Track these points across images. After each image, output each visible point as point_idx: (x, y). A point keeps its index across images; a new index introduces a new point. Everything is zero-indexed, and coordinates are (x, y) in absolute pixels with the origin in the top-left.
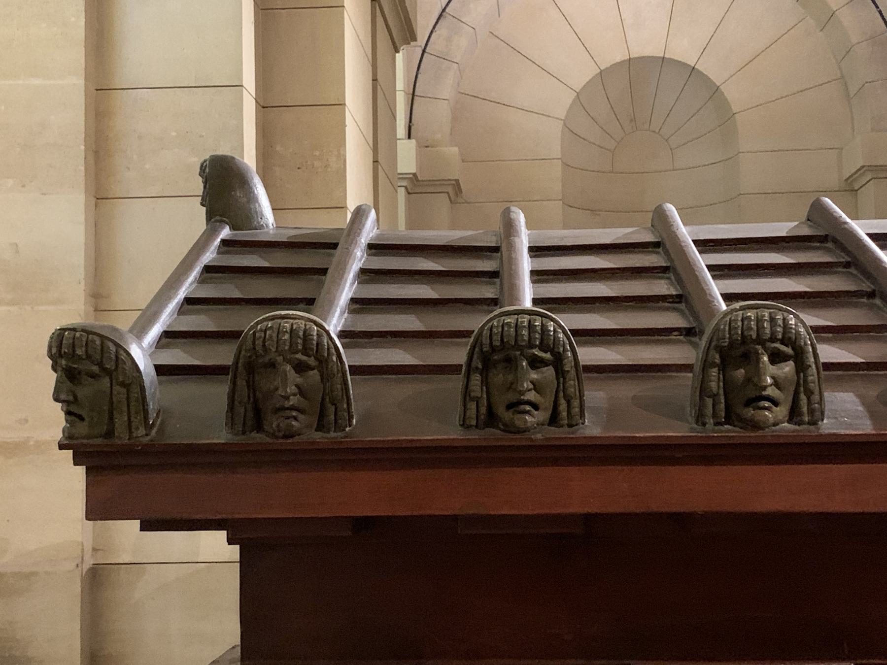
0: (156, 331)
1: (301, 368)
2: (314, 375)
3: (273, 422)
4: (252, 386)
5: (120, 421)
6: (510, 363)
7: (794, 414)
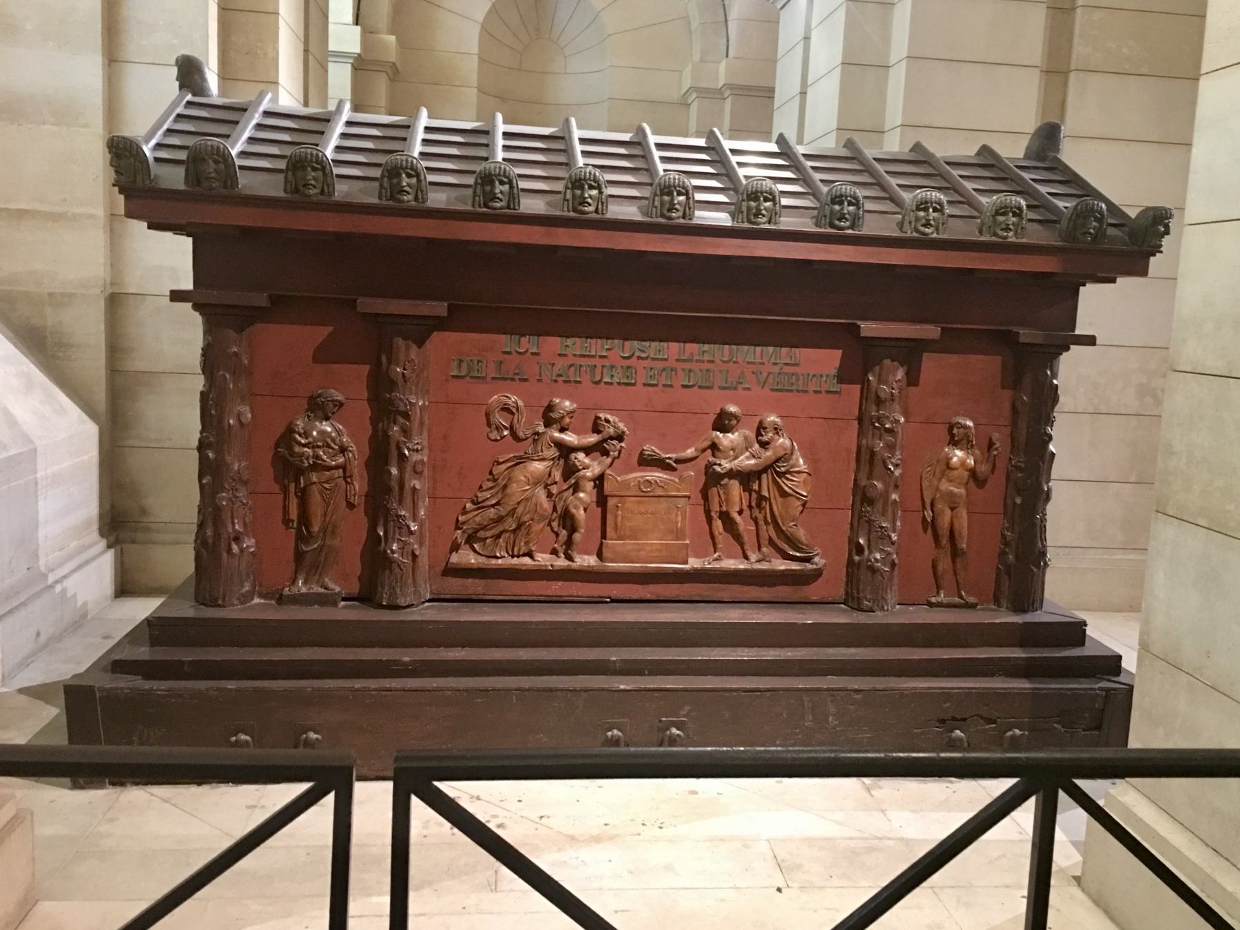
0: (153, 142)
1: (216, 162)
2: (222, 166)
3: (205, 184)
5: (139, 177)
6: (304, 168)
7: (416, 199)
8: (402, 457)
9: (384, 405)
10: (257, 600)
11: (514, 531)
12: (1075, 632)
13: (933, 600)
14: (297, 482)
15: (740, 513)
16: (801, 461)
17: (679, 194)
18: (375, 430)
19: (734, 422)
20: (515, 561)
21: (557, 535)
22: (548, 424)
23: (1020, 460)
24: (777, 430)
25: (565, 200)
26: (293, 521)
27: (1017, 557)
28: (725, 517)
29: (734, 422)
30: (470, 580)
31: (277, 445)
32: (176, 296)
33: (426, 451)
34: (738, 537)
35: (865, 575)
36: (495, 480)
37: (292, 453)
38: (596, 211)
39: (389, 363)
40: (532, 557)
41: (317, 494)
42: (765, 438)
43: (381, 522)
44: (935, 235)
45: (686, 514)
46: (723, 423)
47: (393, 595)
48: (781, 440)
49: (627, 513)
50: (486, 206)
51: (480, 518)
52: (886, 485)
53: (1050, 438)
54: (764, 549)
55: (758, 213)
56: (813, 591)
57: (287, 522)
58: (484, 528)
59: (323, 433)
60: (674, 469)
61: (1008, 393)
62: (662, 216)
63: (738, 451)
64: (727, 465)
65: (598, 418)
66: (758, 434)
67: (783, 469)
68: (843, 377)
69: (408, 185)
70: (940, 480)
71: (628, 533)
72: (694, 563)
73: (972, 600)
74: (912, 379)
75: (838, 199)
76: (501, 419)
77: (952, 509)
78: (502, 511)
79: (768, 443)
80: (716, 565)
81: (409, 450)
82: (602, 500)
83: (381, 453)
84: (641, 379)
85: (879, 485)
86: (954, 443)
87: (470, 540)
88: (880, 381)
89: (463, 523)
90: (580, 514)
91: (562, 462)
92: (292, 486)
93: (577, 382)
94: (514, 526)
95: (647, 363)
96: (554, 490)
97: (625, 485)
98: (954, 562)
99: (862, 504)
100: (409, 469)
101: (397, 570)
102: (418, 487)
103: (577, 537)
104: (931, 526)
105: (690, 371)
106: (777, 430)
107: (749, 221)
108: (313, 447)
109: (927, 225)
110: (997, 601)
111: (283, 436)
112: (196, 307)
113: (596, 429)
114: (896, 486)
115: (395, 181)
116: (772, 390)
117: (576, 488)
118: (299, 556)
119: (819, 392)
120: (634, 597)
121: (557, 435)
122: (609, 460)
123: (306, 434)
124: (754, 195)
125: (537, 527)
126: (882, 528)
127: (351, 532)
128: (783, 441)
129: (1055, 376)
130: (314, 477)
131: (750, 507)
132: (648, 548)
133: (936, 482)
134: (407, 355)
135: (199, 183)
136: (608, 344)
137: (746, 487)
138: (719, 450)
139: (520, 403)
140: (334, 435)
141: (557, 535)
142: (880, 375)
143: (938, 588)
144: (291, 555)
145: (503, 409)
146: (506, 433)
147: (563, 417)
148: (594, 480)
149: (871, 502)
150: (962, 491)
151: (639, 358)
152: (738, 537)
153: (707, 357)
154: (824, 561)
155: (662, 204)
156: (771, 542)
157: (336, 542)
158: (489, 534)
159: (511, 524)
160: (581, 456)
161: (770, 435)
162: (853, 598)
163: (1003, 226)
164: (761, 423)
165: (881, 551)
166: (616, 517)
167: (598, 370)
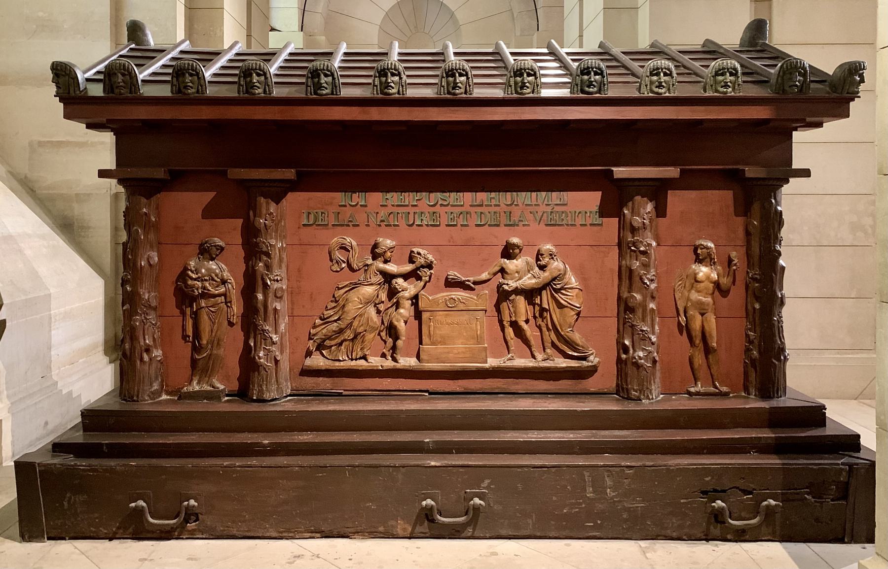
1: (123, 75)
3: (117, 91)
4: (110, 80)
7: (265, 92)
8: (265, 285)
9: (253, 248)
10: (164, 397)
11: (352, 340)
12: (815, 415)
13: (692, 390)
14: (192, 307)
15: (527, 321)
16: (573, 280)
17: (461, 75)
18: (247, 266)
19: (517, 251)
20: (354, 363)
21: (385, 342)
22: (375, 257)
23: (756, 272)
24: (552, 256)
25: (374, 85)
26: (189, 337)
27: (760, 353)
28: (514, 325)
29: (517, 251)
30: (321, 379)
31: (177, 281)
32: (103, 174)
33: (285, 281)
34: (526, 342)
35: (631, 370)
36: (336, 302)
37: (187, 286)
38: (399, 93)
39: (255, 216)
40: (367, 360)
41: (206, 317)
42: (543, 263)
43: (252, 335)
44: (667, 94)
45: (484, 324)
46: (509, 252)
47: (261, 391)
48: (556, 263)
49: (439, 324)
50: (316, 93)
51: (325, 330)
52: (644, 297)
53: (780, 254)
54: (548, 351)
55: (523, 86)
56: (591, 384)
57: (185, 337)
58: (330, 338)
59: (209, 270)
60: (473, 289)
61: (740, 220)
62: (449, 93)
63: (522, 273)
64: (511, 284)
65: (412, 252)
66: (538, 260)
67: (559, 286)
68: (604, 211)
69: (258, 82)
70: (689, 291)
71: (439, 340)
72: (492, 362)
73: (725, 389)
74: (661, 211)
75: (586, 71)
76: (339, 255)
77: (702, 315)
78: (342, 324)
79: (545, 266)
80: (509, 364)
81: (270, 279)
82: (418, 315)
83: (251, 283)
84: (444, 220)
85: (638, 297)
86: (699, 260)
87: (320, 347)
88: (633, 213)
89: (314, 335)
90: (401, 326)
91: (387, 286)
92: (188, 311)
93: (395, 225)
94: (352, 336)
95: (449, 209)
96: (382, 307)
97: (435, 302)
98: (707, 358)
99: (625, 313)
100: (271, 295)
101: (263, 372)
102: (278, 308)
103: (400, 343)
104: (685, 329)
105: (481, 213)
106: (552, 256)
107: (517, 93)
108: (202, 281)
109: (660, 86)
110: (746, 389)
111: (182, 272)
112: (121, 181)
113: (411, 260)
114: (653, 298)
115: (249, 79)
116: (547, 225)
117: (397, 305)
118: (194, 363)
119: (585, 225)
120: (447, 390)
121: (382, 266)
122: (422, 284)
123: (197, 271)
124: (519, 73)
125: (369, 336)
126: (642, 331)
127: (231, 345)
128: (557, 265)
129: (778, 203)
130: (203, 303)
131: (535, 317)
132: (455, 351)
133: (687, 294)
134: (268, 209)
135: (113, 92)
136: (419, 195)
137: (531, 302)
138: (507, 273)
139: (354, 243)
140: (222, 272)
141: (385, 342)
142: (633, 209)
143: (696, 380)
144: (187, 362)
145: (341, 248)
146: (344, 265)
147: (385, 252)
148: (411, 299)
149: (632, 310)
150: (709, 300)
151: (441, 205)
152: (526, 342)
153: (494, 202)
154: (597, 360)
155: (448, 84)
156: (553, 345)
157: (221, 352)
158: (333, 343)
159: (349, 334)
160: (400, 281)
161: (547, 259)
162: (623, 389)
163: (723, 84)
164: (539, 251)
165: (643, 350)
166: (429, 327)
167: (411, 216)
